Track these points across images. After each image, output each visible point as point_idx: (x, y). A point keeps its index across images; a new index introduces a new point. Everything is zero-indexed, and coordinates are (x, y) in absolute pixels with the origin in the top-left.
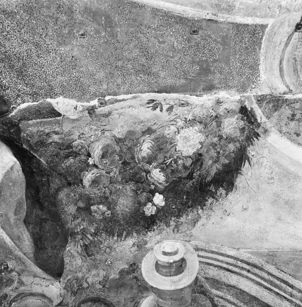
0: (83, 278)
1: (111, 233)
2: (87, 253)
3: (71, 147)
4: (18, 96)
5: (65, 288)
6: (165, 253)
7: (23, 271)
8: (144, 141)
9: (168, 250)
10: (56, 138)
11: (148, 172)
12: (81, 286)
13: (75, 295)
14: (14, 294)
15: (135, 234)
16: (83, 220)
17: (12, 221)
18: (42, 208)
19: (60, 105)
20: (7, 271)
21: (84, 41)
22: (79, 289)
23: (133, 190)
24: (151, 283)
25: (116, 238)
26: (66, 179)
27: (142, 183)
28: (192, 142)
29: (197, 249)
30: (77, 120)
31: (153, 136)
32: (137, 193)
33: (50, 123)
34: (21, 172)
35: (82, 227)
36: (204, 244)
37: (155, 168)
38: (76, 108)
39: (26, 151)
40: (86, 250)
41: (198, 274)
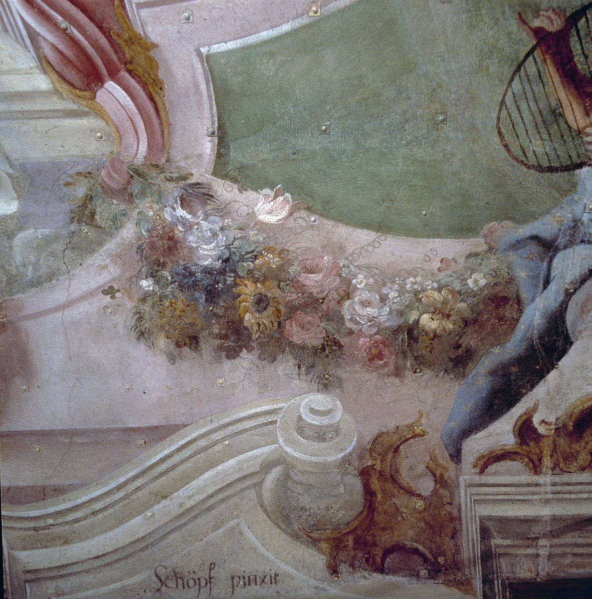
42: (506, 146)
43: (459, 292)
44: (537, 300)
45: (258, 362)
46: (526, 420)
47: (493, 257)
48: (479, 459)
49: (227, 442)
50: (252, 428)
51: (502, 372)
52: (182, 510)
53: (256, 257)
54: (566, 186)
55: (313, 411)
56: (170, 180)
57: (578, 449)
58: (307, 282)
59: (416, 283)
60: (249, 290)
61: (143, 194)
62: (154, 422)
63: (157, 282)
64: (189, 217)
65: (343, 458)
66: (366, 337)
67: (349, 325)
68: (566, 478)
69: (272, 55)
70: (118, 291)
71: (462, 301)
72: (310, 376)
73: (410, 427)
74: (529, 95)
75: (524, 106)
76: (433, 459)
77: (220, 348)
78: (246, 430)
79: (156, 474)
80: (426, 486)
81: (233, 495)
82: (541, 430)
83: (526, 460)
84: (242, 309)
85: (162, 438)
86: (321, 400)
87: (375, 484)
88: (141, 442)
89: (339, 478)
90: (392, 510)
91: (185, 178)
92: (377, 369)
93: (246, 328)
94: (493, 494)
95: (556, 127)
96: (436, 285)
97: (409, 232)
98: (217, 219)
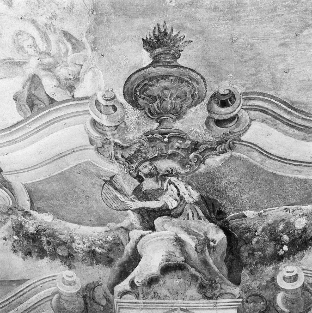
0: (249, 285)
1: (263, 264)
2: (252, 274)
3: (249, 229)
4: (231, 211)
5: (241, 290)
6: (288, 272)
7: (222, 283)
8: (280, 224)
9: (289, 271)
10: (243, 226)
11: (281, 236)
12: (249, 288)
13: (246, 293)
14: (219, 294)
15: (274, 264)
16: (250, 258)
17: (219, 261)
18: (233, 254)
19: (247, 213)
20: (215, 283)
21: (260, 189)
22: (248, 290)
23: (274, 244)
24: (281, 286)
25: (265, 266)
26: (245, 242)
27: (278, 241)
28: (302, 223)
29: (303, 270)
30: (253, 218)
31: (285, 222)
32: (275, 245)
33: (241, 220)
34: (226, 240)
35: (250, 262)
36: (306, 267)
37: (285, 235)
38: (254, 214)
39: (230, 231)
40: (251, 272)
41: (304, 281)
42: (106, 204)
43: (105, 241)
44: (128, 244)
45: (50, 261)
46: (133, 281)
47: (112, 232)
48: (119, 294)
49: (41, 286)
50: (49, 281)
51: (122, 265)
52: (26, 308)
53: (45, 231)
54: (126, 214)
55: (67, 276)
56: (19, 210)
57: (150, 291)
58: (61, 237)
59: (92, 238)
60: (44, 239)
61: (12, 214)
62: (19, 278)
63: (18, 237)
64: (25, 220)
65: (77, 292)
66: (80, 254)
67: (75, 250)
68: (147, 301)
69: (40, 184)
70: (7, 239)
71: (106, 244)
72: (66, 265)
73: (97, 282)
74: (108, 193)
75: (108, 196)
76: (105, 293)
77: (38, 256)
78: (47, 282)
79: (19, 296)
80: (104, 302)
81: (43, 304)
82: (138, 284)
83: (134, 294)
84: (43, 245)
85: (21, 284)
86: (70, 273)
87: (88, 301)
88: (15, 285)
89: (76, 298)
90: (93, 310)
91: (23, 210)
92: (85, 263)
93: (45, 250)
94: (125, 306)
95: (117, 200)
96: (98, 239)
97: (87, 225)
98: (33, 220)
